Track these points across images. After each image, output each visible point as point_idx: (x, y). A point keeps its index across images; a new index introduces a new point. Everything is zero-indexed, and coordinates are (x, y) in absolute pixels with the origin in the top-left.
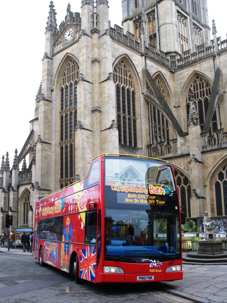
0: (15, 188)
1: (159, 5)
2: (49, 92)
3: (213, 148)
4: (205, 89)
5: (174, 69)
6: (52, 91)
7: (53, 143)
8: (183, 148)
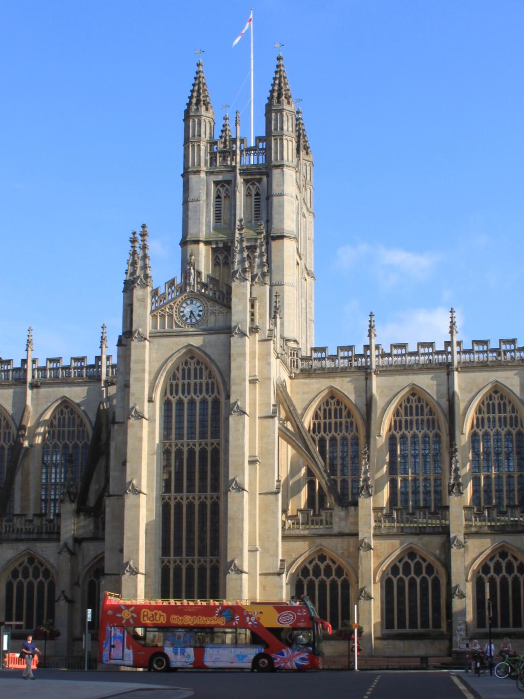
4: (344, 420)
8: (343, 523)
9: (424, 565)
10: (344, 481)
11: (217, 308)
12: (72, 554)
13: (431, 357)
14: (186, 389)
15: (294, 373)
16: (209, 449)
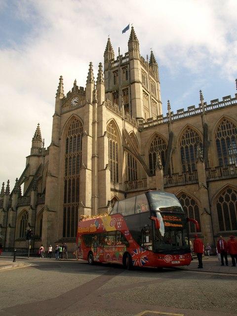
0: (14, 209)
1: (131, 86)
2: (58, 140)
3: (172, 185)
6: (60, 139)
7: (60, 177)
8: (151, 184)
9: (190, 200)
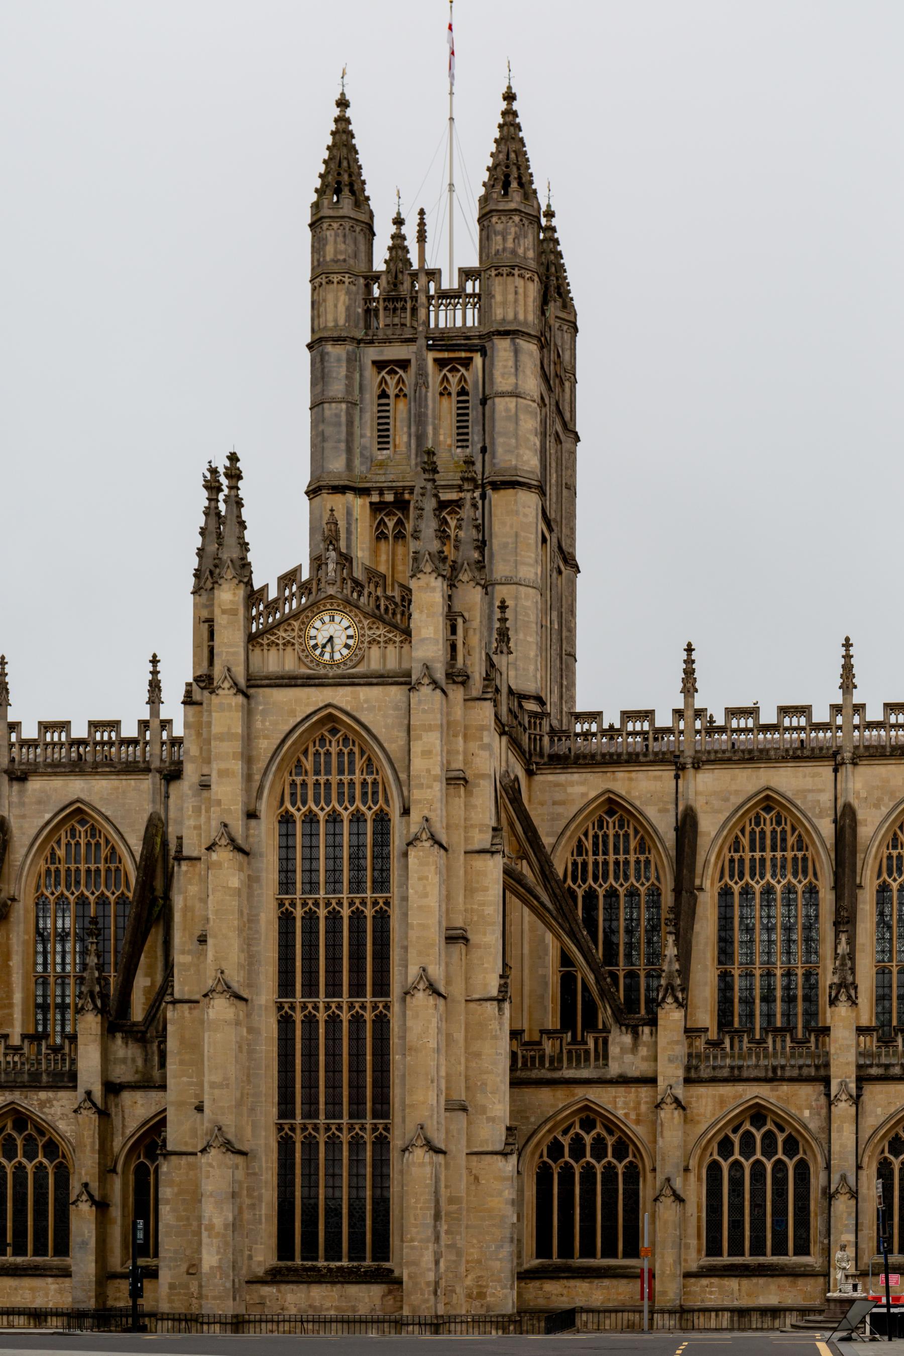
4: (632, 858)
5: (537, 764)
10: (632, 975)
11: (381, 631)
12: (104, 1114)
13: (803, 736)
14: (323, 792)
15: (537, 764)
16: (369, 912)
